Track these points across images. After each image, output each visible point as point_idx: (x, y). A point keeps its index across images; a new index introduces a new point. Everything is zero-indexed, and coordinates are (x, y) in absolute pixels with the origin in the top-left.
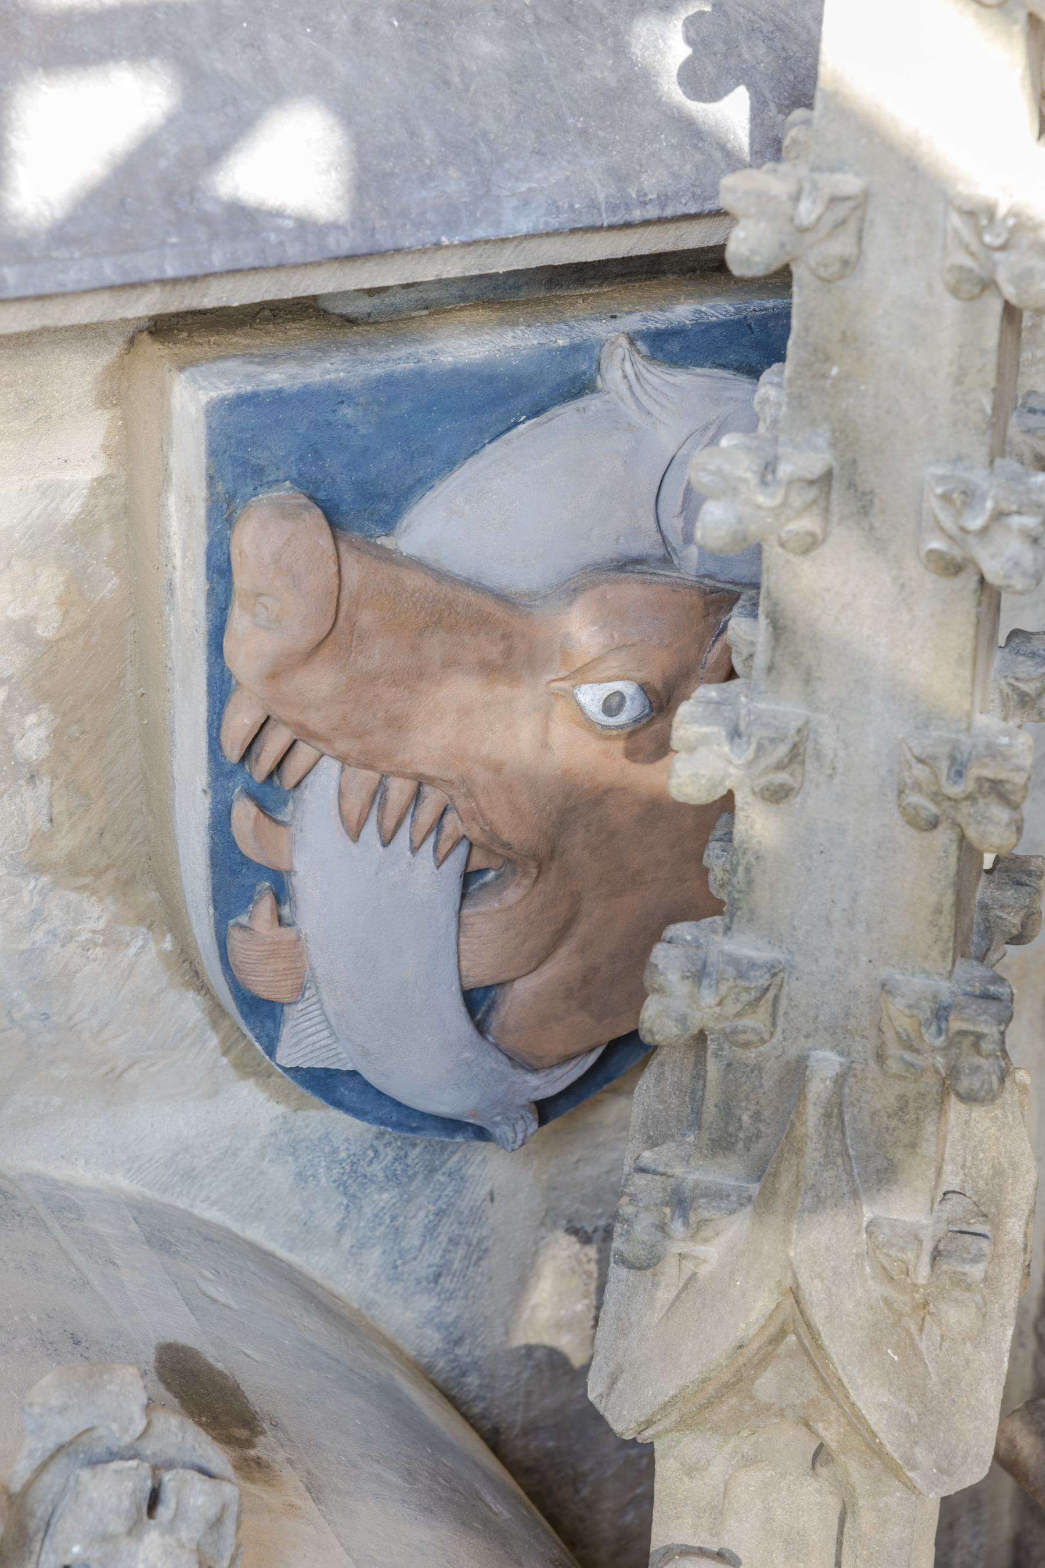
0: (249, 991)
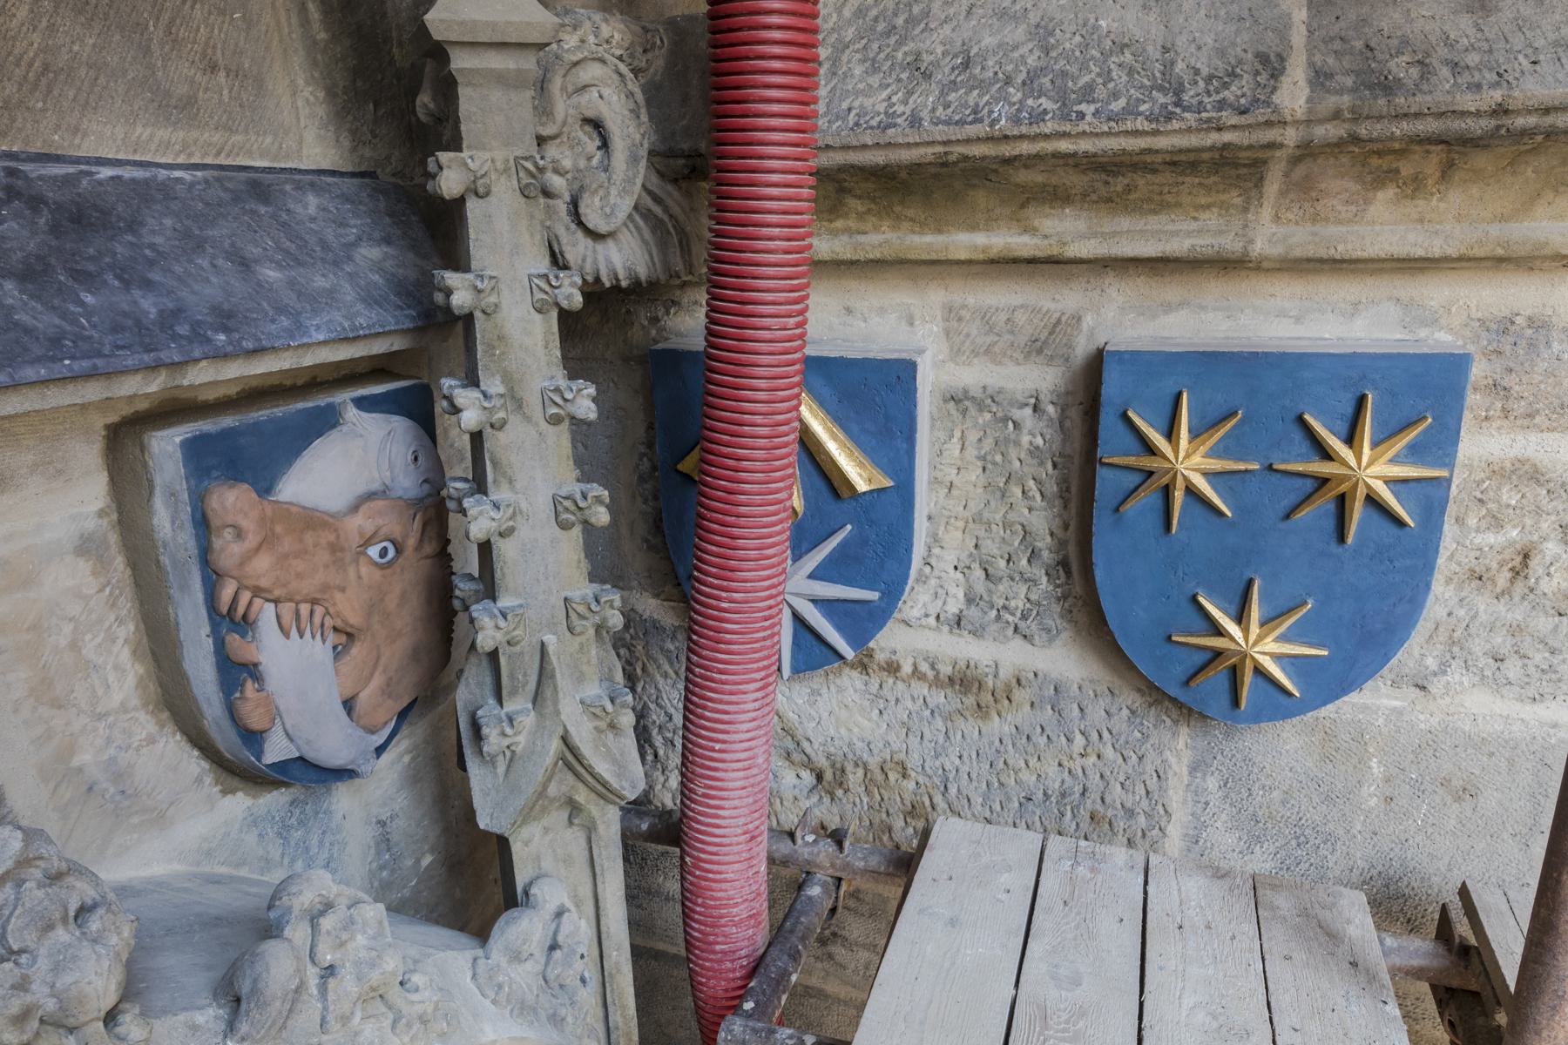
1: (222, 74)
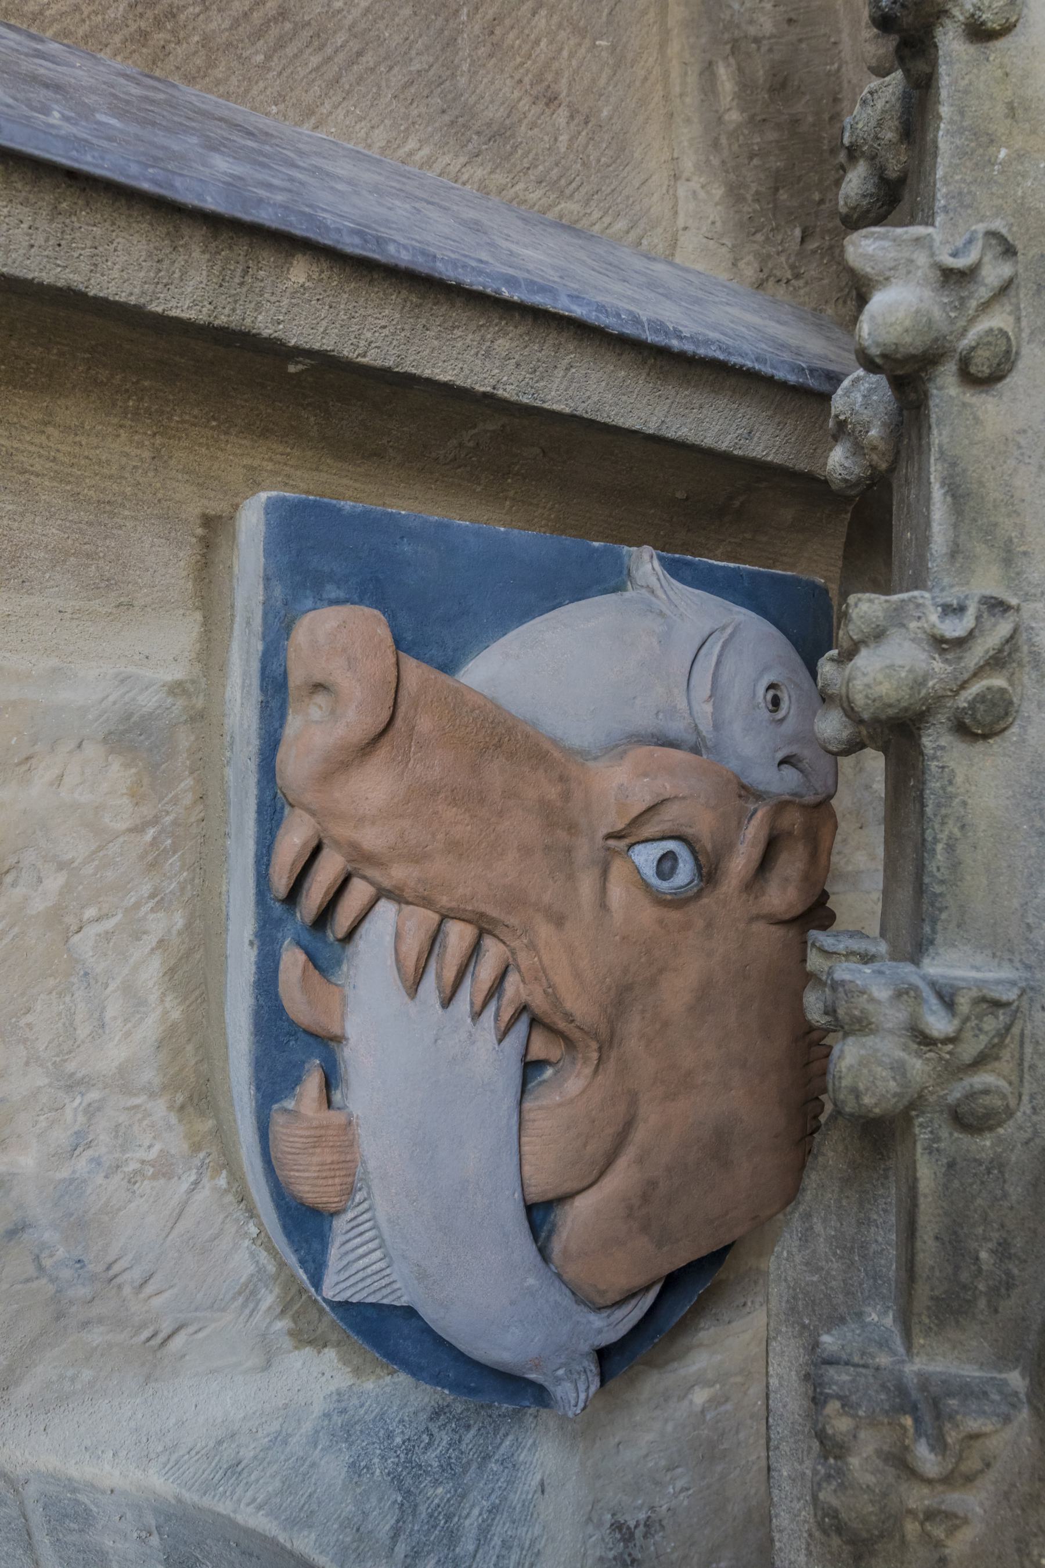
0: (295, 1198)
1: (561, 116)
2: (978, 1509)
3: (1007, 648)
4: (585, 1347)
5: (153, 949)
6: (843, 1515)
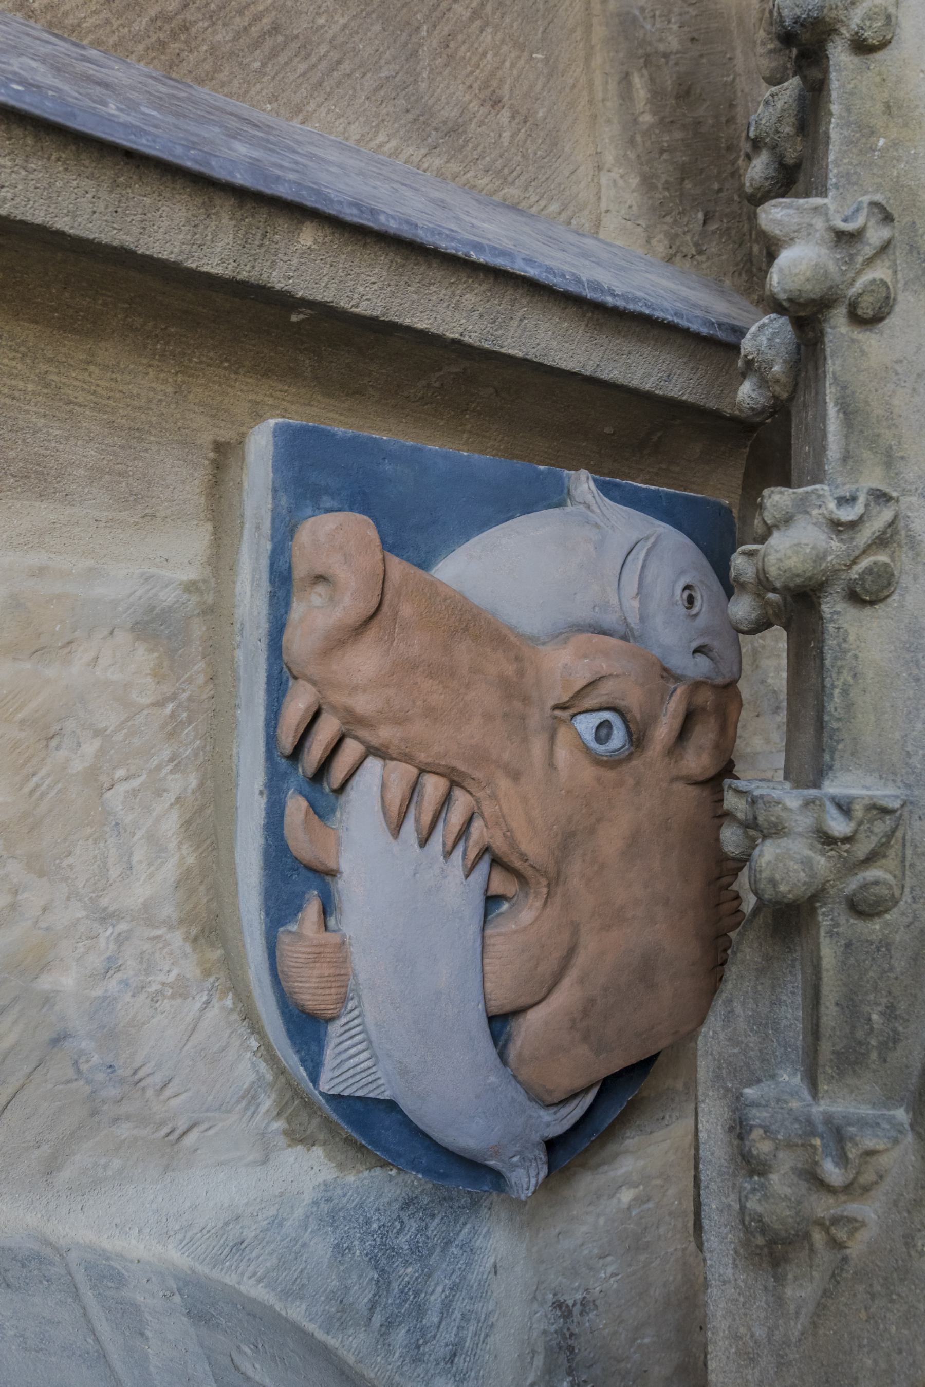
0: (297, 1005)
1: (504, 116)
2: (873, 1216)
3: (889, 530)
4: (536, 1137)
5: (171, 805)
6: (766, 1219)
